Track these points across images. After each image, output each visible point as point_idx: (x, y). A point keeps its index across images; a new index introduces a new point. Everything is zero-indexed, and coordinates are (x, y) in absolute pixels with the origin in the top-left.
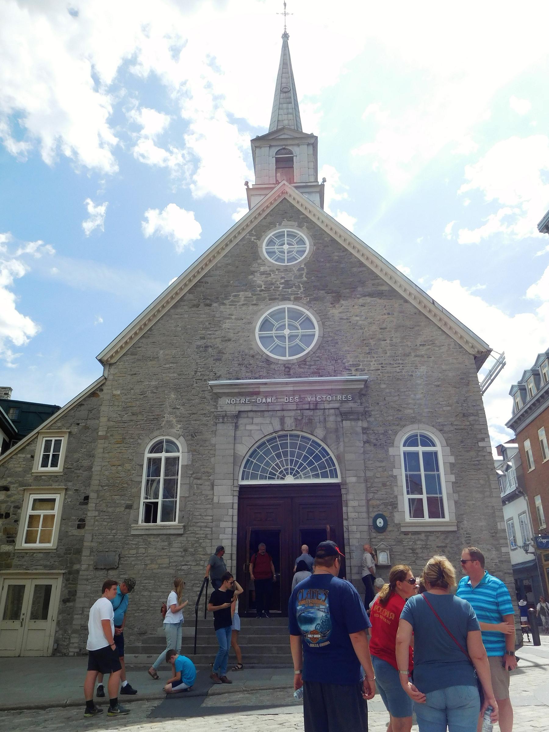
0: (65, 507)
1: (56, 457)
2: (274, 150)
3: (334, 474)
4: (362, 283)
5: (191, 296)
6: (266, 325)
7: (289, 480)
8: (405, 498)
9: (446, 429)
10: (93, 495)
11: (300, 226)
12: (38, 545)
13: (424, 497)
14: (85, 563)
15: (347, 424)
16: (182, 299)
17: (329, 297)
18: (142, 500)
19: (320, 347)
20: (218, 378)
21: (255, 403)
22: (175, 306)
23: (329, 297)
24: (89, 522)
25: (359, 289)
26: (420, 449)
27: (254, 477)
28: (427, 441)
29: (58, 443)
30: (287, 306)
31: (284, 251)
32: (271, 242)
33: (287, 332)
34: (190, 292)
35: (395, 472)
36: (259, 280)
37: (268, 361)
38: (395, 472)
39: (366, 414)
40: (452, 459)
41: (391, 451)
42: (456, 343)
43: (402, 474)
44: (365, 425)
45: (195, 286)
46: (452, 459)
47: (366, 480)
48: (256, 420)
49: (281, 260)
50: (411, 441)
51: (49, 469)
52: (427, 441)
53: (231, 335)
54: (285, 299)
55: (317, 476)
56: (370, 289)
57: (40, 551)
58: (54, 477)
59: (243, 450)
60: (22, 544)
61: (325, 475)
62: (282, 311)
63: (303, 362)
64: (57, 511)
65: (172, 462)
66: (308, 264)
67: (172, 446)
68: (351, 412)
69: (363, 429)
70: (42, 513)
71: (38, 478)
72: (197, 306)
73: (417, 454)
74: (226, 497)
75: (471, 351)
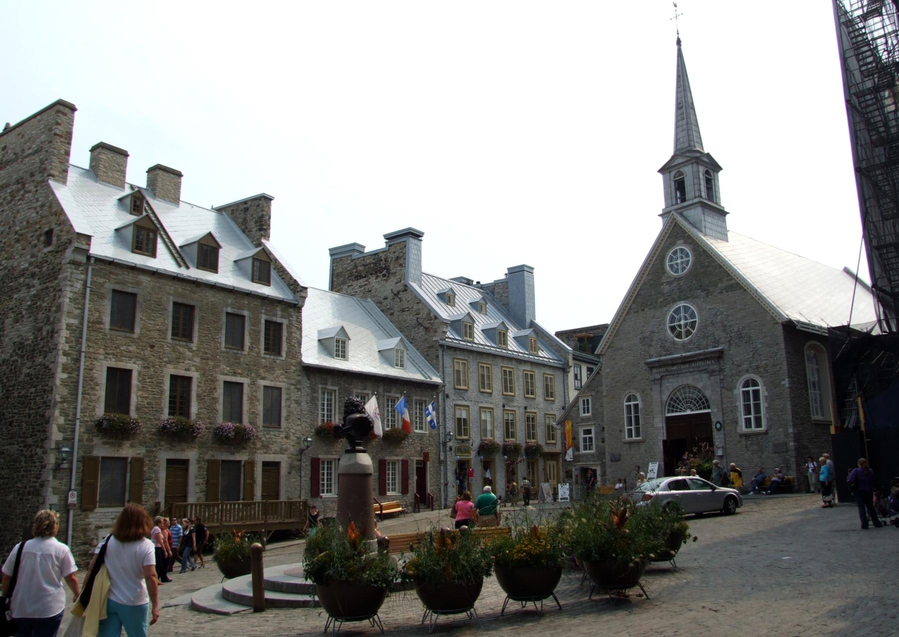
0: (596, 433)
1: (588, 408)
2: (673, 173)
3: (709, 408)
4: (721, 280)
5: (634, 306)
6: (672, 319)
7: (689, 412)
8: (742, 418)
9: (765, 375)
10: (606, 426)
11: (685, 243)
12: (588, 451)
13: (752, 416)
14: (608, 458)
15: (712, 378)
16: (630, 309)
17: (703, 294)
18: (626, 428)
19: (699, 330)
20: (651, 356)
21: (667, 371)
22: (628, 314)
23: (703, 294)
24: (606, 439)
25: (719, 285)
26: (751, 389)
27: (673, 411)
28: (755, 383)
29: (588, 401)
30: (681, 304)
31: (680, 263)
32: (671, 259)
33: (682, 322)
34: (633, 303)
35: (737, 404)
36: (666, 288)
37: (674, 343)
38: (737, 404)
39: (721, 370)
40: (766, 394)
41: (736, 392)
42: (772, 317)
43: (741, 404)
44: (722, 377)
45: (636, 298)
46: (766, 394)
47: (722, 409)
48: (671, 380)
49: (677, 271)
50: (746, 384)
51: (586, 415)
52: (755, 383)
53: (655, 329)
54: (680, 299)
55: (701, 409)
56: (725, 284)
57: (589, 454)
58: (588, 419)
59: (665, 398)
60: (582, 451)
61: (705, 408)
62: (679, 308)
63: (691, 341)
64: (593, 435)
65: (636, 406)
66: (691, 272)
67: (635, 399)
68: (713, 371)
69: (721, 380)
70: (588, 436)
71: (583, 420)
72: (637, 312)
73: (748, 392)
74: (659, 424)
75: (780, 321)
